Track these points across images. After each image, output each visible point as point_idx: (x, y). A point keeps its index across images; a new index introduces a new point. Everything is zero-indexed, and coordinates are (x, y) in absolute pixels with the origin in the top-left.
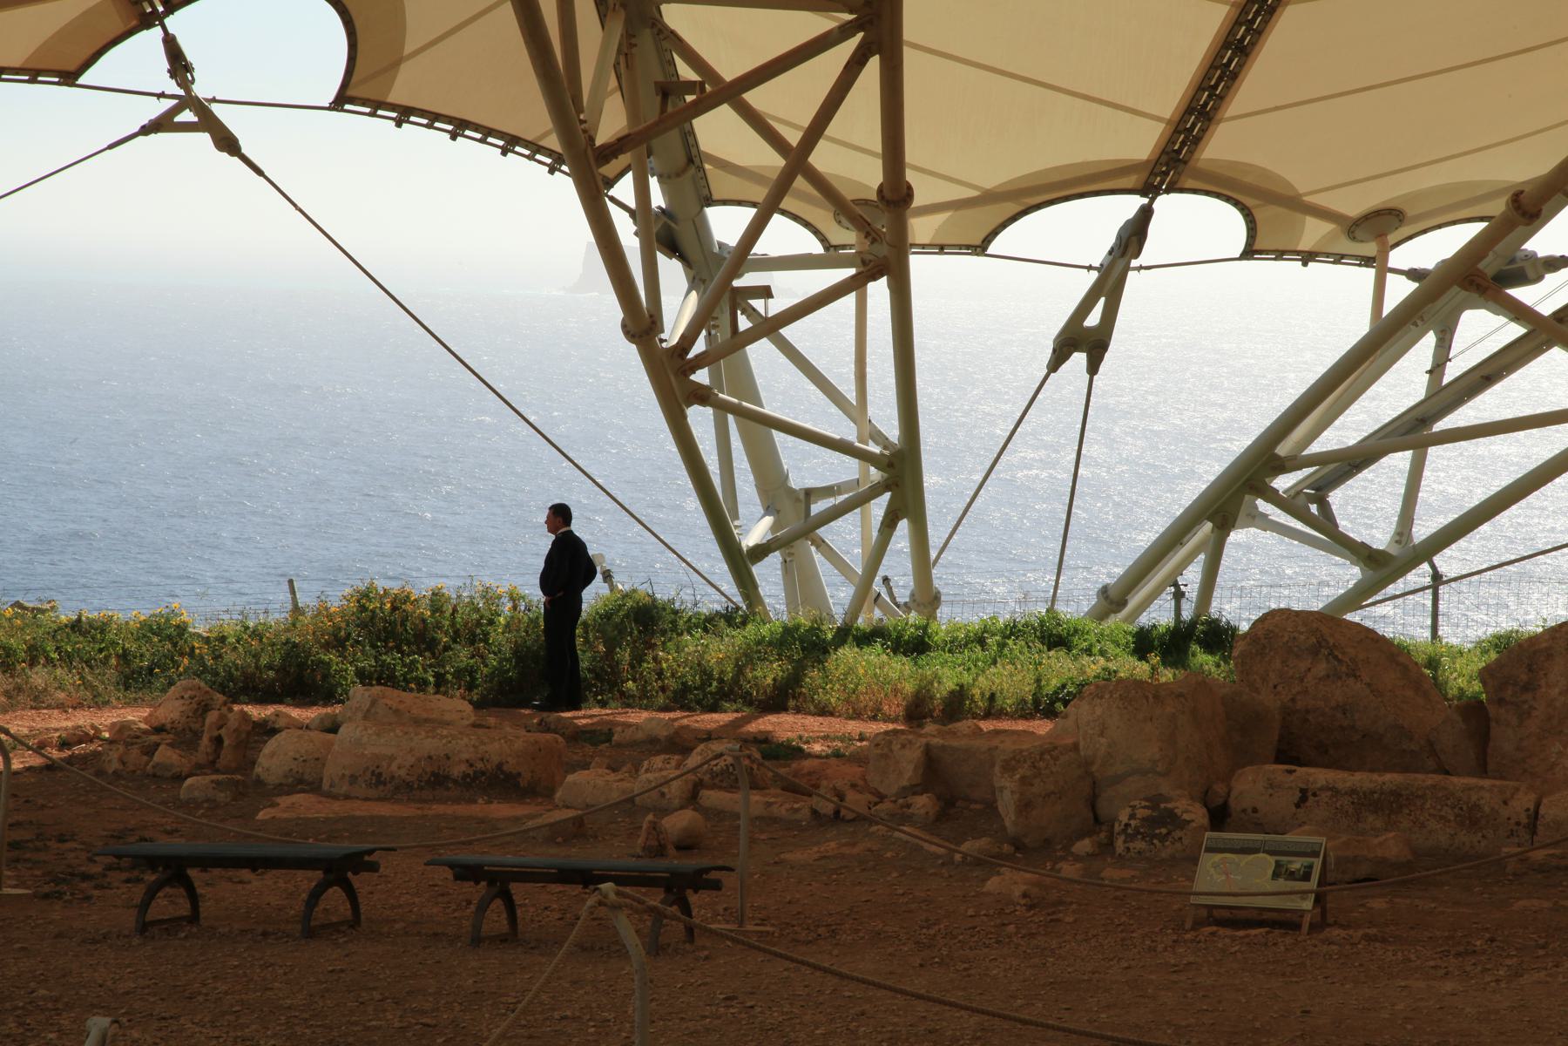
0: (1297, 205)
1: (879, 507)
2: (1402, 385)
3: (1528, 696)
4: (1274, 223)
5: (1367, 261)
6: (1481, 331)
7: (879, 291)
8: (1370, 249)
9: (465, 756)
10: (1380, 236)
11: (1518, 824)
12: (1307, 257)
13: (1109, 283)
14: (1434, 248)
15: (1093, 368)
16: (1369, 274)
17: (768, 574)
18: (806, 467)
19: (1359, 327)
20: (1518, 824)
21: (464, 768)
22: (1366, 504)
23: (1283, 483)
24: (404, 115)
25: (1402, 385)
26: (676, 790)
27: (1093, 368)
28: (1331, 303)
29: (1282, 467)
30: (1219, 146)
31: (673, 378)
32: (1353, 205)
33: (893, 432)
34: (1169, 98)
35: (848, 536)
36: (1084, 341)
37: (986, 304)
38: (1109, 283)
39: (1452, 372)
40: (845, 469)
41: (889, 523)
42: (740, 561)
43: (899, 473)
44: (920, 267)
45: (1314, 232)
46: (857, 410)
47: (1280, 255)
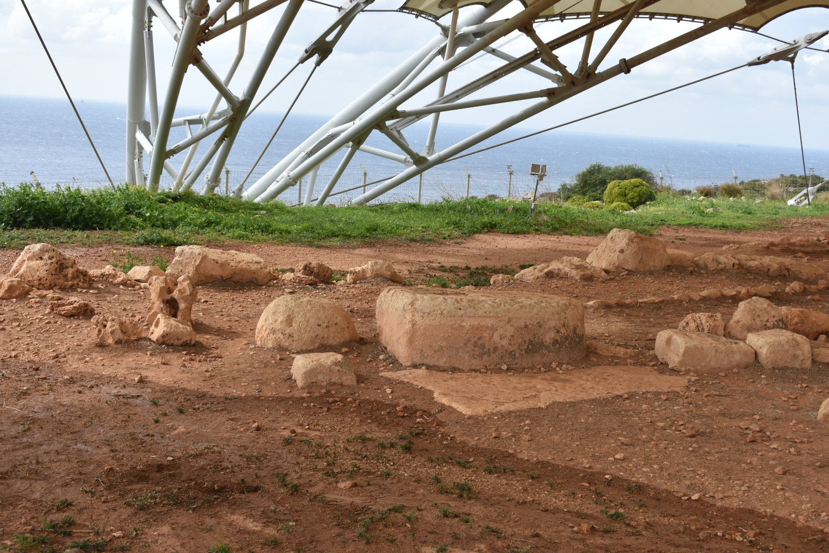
9: (552, 323)
15: (318, 64)
21: (552, 334)
22: (416, 133)
27: (318, 64)
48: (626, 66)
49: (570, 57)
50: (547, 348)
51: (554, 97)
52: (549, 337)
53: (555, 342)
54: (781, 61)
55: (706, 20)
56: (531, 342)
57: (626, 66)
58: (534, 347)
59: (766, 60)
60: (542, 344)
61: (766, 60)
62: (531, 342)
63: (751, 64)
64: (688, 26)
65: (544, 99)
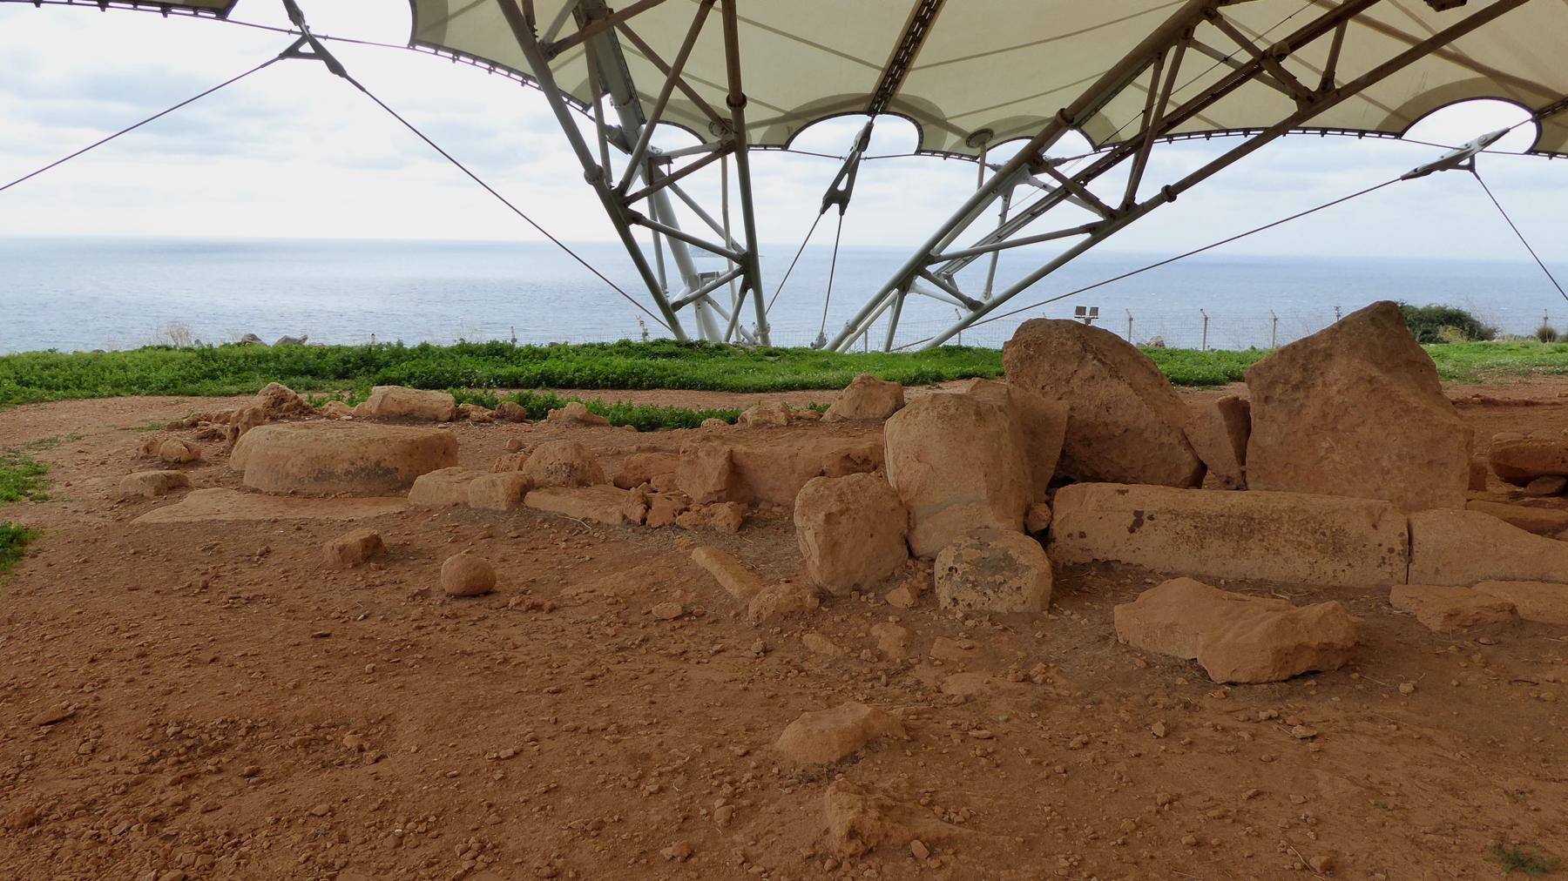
0: (945, 125)
1: (739, 280)
2: (986, 223)
3: (1300, 394)
4: (934, 133)
5: (974, 159)
6: (1025, 195)
7: (732, 158)
8: (976, 151)
9: (346, 456)
10: (983, 143)
11: (1391, 551)
12: (947, 155)
13: (850, 168)
14: (1005, 153)
15: (842, 212)
16: (976, 166)
17: (687, 316)
18: (704, 263)
19: (971, 190)
20: (1391, 551)
21: (346, 465)
22: (971, 280)
23: (932, 269)
24: (457, 54)
25: (986, 223)
26: (500, 499)
27: (842, 212)
28: (958, 179)
29: (933, 261)
30: (910, 87)
31: (618, 206)
32: (971, 126)
33: (742, 242)
34: (883, 52)
35: (724, 296)
36: (837, 197)
37: (787, 180)
38: (850, 168)
39: (1010, 216)
40: (721, 265)
41: (744, 290)
42: (669, 310)
43: (748, 264)
44: (754, 157)
45: (951, 140)
46: (725, 233)
47: (933, 153)
48: (1169, 194)
49: (1110, 188)
50: (338, 477)
51: (1097, 232)
52: (339, 469)
53: (348, 472)
54: (1449, 171)
55: (1265, 129)
56: (320, 471)
57: (1169, 194)
58: (323, 475)
59: (1427, 171)
60: (331, 474)
61: (1427, 171)
62: (320, 471)
63: (1404, 178)
64: (1239, 140)
65: (1088, 235)
